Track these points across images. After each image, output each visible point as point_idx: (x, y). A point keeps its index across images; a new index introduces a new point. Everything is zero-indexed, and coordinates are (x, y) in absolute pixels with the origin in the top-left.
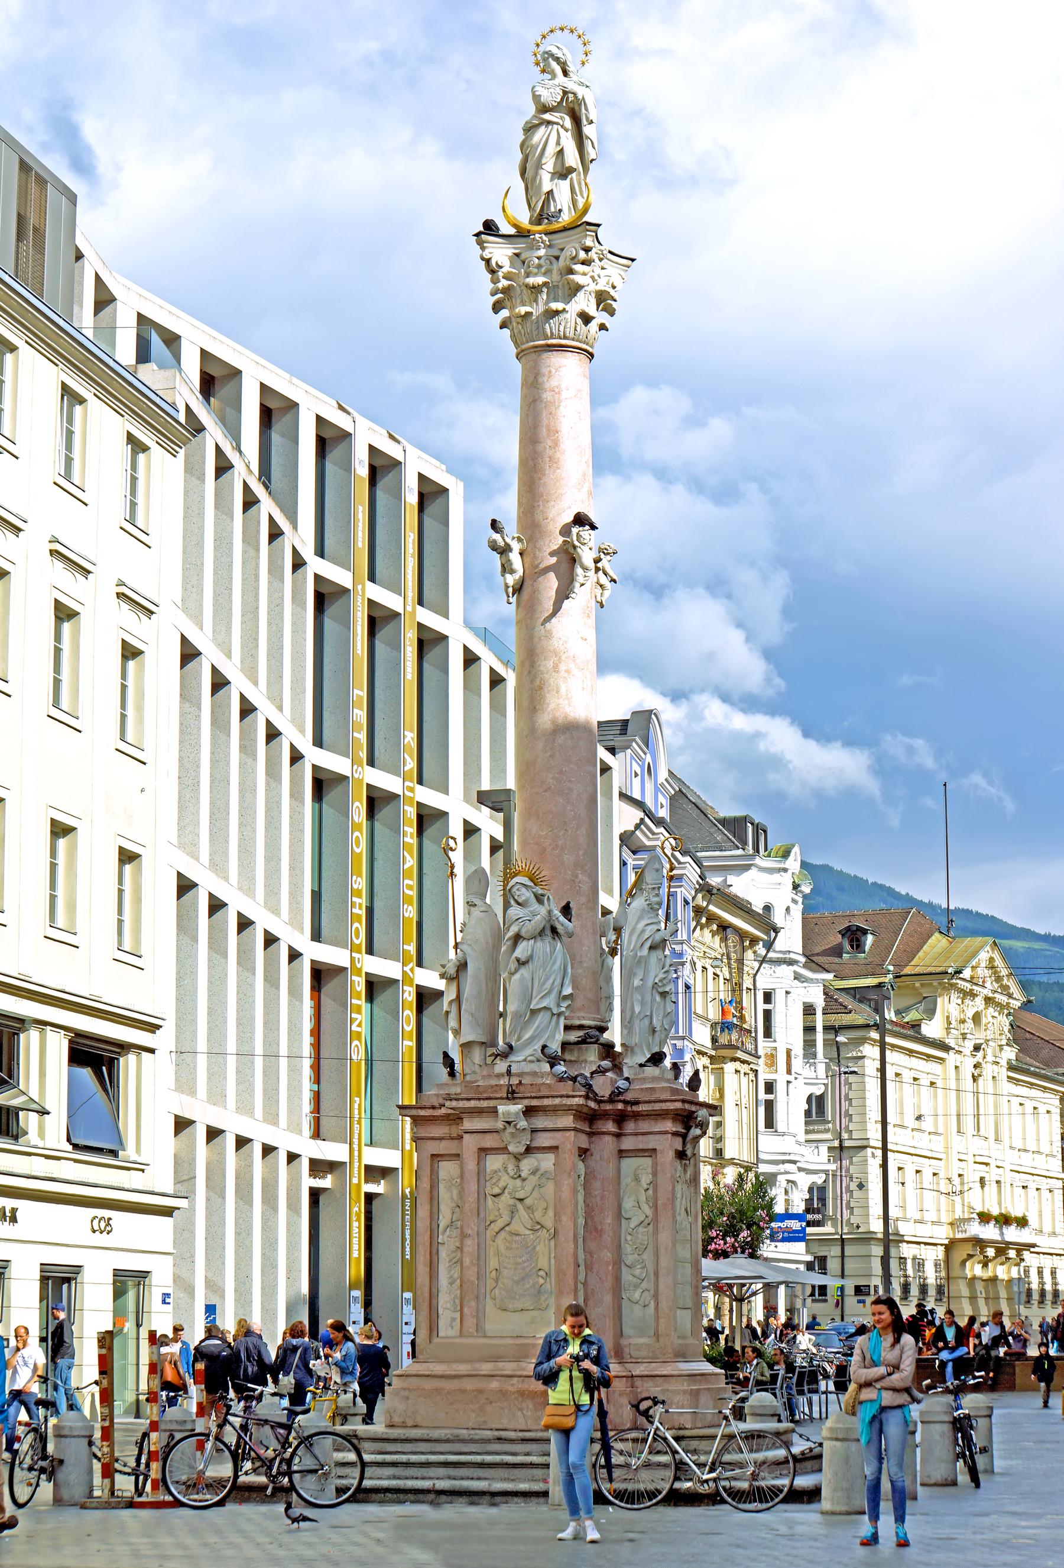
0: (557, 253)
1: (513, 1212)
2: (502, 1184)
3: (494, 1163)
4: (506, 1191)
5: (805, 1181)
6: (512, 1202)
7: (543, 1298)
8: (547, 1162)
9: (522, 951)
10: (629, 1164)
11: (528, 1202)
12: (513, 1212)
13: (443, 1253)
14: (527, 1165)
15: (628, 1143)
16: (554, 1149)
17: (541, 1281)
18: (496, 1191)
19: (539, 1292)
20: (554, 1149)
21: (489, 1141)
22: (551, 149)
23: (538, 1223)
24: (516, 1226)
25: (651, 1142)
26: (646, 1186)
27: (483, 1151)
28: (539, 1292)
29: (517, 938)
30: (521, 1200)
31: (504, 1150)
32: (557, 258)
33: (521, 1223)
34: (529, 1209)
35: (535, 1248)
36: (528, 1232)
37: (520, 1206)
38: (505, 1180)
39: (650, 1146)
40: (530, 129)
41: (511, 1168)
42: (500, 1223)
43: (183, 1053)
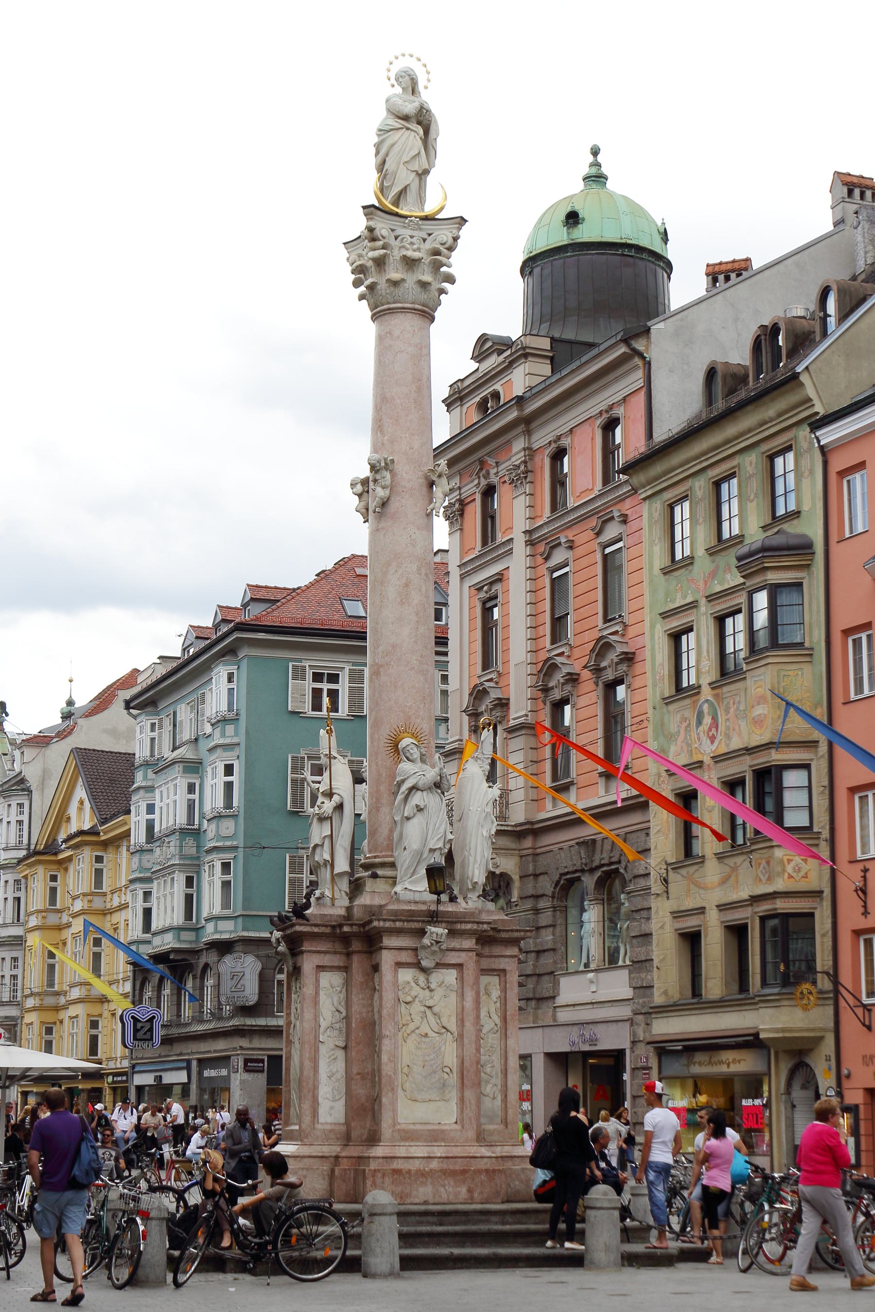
0: (426, 236)
2: (413, 993)
4: (417, 1000)
6: (423, 1009)
7: (447, 1091)
8: (451, 976)
9: (417, 798)
10: (485, 980)
11: (436, 1009)
12: (424, 1015)
14: (436, 977)
16: (459, 966)
17: (446, 1076)
18: (409, 999)
19: (444, 1085)
20: (459, 966)
23: (444, 1028)
25: (502, 964)
26: (495, 1000)
28: (444, 1085)
29: (414, 788)
30: (430, 1007)
32: (424, 240)
35: (440, 1048)
36: (435, 1035)
37: (428, 1012)
38: (416, 990)
39: (501, 967)
42: (412, 1026)
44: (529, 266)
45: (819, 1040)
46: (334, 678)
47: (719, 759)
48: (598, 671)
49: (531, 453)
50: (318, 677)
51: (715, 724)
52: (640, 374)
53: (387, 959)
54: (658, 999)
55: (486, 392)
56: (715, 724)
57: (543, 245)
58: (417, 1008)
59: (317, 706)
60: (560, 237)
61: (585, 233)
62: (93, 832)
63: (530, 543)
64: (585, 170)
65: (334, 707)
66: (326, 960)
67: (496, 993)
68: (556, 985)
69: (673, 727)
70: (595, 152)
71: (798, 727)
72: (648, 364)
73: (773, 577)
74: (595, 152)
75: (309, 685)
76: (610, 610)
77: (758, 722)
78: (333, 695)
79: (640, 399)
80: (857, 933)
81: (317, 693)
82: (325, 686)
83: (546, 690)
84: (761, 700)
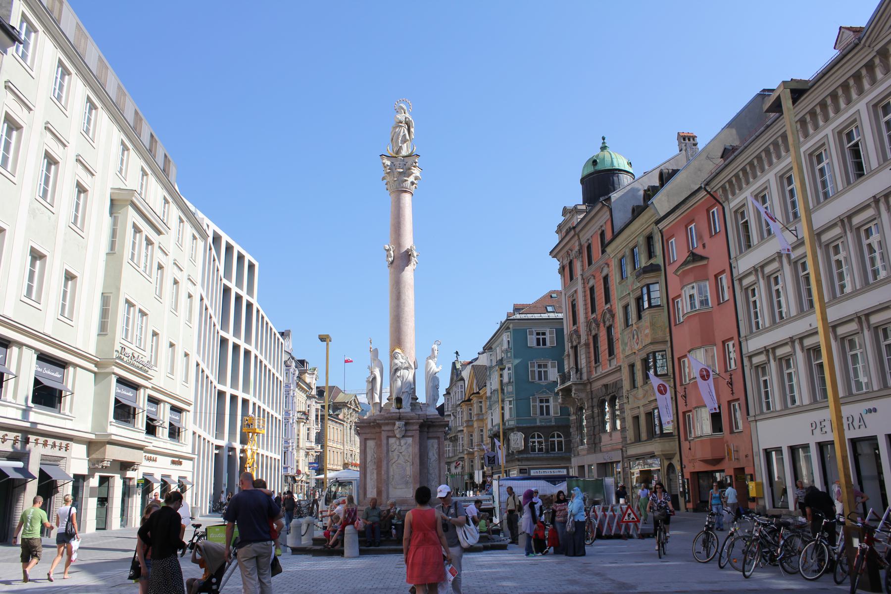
1: (399, 456)
3: (392, 441)
5: (315, 454)
8: (410, 440)
10: (430, 442)
12: (399, 456)
13: (368, 470)
14: (403, 442)
15: (430, 435)
20: (412, 436)
21: (390, 434)
22: (402, 134)
24: (399, 461)
25: (439, 434)
27: (388, 437)
31: (395, 436)
33: (401, 461)
34: (404, 456)
40: (395, 128)
41: (398, 443)
43: (195, 412)
44: (583, 181)
45: (674, 454)
46: (544, 334)
47: (639, 350)
48: (604, 322)
49: (581, 245)
50: (538, 334)
51: (638, 338)
52: (608, 213)
53: (384, 435)
54: (629, 442)
55: (567, 227)
56: (638, 338)
57: (586, 173)
58: (396, 453)
59: (538, 344)
60: (591, 169)
61: (599, 167)
62: (478, 393)
63: (583, 279)
64: (601, 145)
65: (544, 344)
66: (368, 436)
67: (436, 446)
68: (600, 438)
69: (626, 341)
70: (604, 139)
71: (660, 335)
72: (611, 210)
73: (648, 281)
74: (604, 139)
75: (534, 337)
76: (607, 300)
77: (646, 335)
78: (544, 340)
79: (609, 223)
80: (684, 413)
81: (538, 340)
82: (541, 337)
83: (590, 330)
84: (647, 327)
